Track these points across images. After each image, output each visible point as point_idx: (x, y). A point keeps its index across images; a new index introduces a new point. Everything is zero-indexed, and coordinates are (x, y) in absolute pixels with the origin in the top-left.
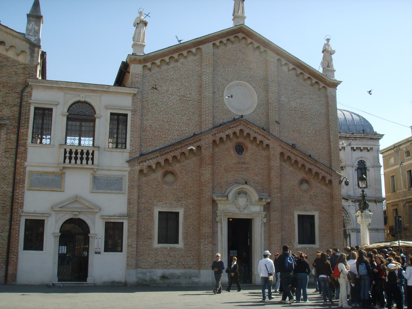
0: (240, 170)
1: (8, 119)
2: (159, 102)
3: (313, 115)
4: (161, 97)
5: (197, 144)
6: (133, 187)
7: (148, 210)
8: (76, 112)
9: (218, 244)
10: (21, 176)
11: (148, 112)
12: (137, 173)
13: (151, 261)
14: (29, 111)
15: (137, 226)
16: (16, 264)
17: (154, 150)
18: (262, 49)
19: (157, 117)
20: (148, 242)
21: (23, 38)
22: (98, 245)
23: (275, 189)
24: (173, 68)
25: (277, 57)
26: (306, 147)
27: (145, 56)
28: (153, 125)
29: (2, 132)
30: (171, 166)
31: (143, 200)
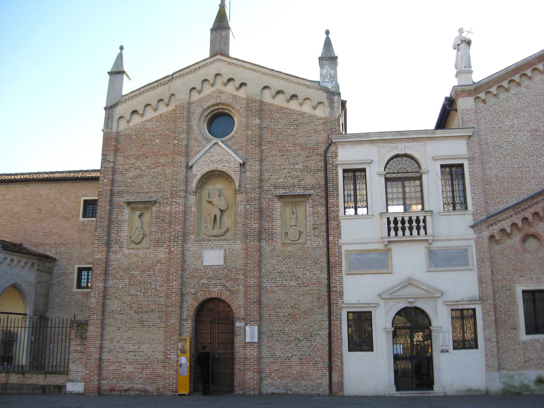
1: (313, 188)
2: (503, 143)
4: (505, 136)
6: (483, 260)
7: (507, 290)
8: (395, 169)
10: (337, 258)
11: (491, 159)
12: (486, 241)
13: (519, 359)
14: (337, 175)
15: (495, 312)
16: (342, 370)
17: (505, 207)
19: (503, 163)
20: (512, 333)
21: (318, 87)
22: (444, 341)
27: (475, 85)
28: (499, 174)
29: (307, 204)
30: (532, 227)
31: (499, 277)
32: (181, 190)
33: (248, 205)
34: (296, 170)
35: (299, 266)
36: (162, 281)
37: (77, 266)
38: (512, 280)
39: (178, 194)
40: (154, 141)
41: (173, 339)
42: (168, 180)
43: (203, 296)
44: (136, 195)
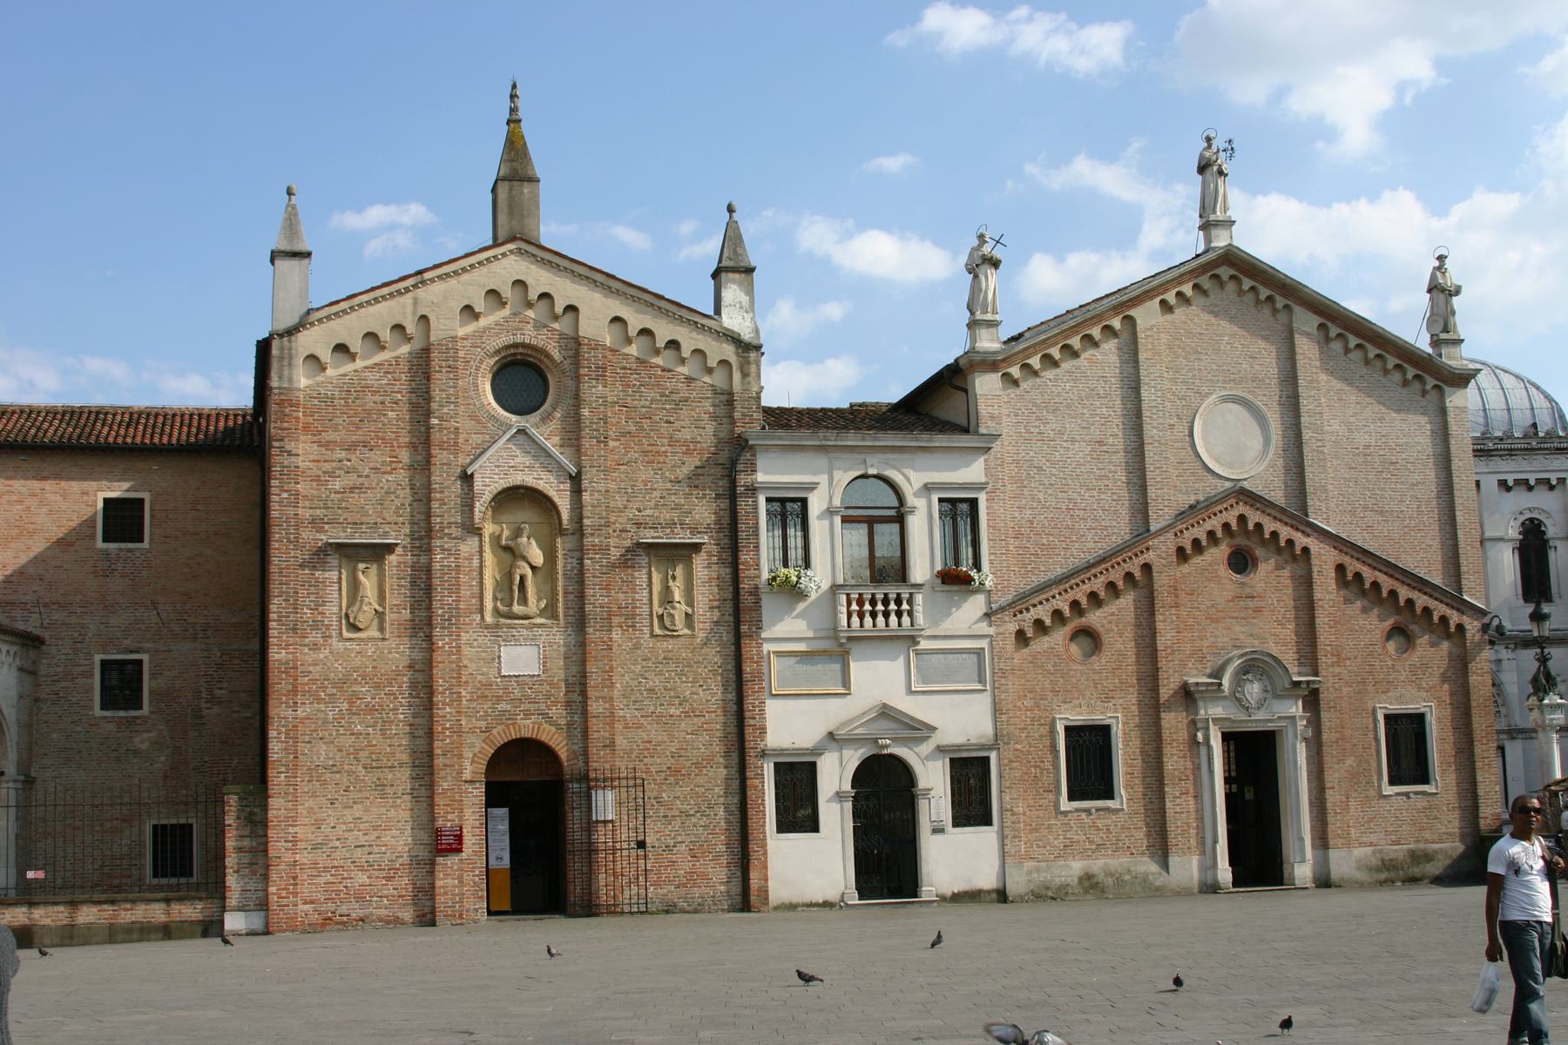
0: (1243, 615)
3: (1411, 463)
5: (1141, 560)
6: (1004, 673)
7: (1041, 725)
9: (1202, 796)
16: (766, 867)
18: (1280, 302)
23: (1329, 655)
24: (1069, 372)
25: (1316, 320)
26: (1397, 546)
32: (452, 523)
33: (588, 559)
34: (675, 494)
35: (684, 679)
36: (419, 706)
37: (98, 658)
38: (1049, 708)
39: (446, 531)
40: (384, 415)
41: (449, 818)
42: (420, 500)
43: (503, 735)
44: (351, 528)
